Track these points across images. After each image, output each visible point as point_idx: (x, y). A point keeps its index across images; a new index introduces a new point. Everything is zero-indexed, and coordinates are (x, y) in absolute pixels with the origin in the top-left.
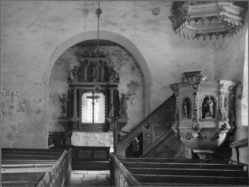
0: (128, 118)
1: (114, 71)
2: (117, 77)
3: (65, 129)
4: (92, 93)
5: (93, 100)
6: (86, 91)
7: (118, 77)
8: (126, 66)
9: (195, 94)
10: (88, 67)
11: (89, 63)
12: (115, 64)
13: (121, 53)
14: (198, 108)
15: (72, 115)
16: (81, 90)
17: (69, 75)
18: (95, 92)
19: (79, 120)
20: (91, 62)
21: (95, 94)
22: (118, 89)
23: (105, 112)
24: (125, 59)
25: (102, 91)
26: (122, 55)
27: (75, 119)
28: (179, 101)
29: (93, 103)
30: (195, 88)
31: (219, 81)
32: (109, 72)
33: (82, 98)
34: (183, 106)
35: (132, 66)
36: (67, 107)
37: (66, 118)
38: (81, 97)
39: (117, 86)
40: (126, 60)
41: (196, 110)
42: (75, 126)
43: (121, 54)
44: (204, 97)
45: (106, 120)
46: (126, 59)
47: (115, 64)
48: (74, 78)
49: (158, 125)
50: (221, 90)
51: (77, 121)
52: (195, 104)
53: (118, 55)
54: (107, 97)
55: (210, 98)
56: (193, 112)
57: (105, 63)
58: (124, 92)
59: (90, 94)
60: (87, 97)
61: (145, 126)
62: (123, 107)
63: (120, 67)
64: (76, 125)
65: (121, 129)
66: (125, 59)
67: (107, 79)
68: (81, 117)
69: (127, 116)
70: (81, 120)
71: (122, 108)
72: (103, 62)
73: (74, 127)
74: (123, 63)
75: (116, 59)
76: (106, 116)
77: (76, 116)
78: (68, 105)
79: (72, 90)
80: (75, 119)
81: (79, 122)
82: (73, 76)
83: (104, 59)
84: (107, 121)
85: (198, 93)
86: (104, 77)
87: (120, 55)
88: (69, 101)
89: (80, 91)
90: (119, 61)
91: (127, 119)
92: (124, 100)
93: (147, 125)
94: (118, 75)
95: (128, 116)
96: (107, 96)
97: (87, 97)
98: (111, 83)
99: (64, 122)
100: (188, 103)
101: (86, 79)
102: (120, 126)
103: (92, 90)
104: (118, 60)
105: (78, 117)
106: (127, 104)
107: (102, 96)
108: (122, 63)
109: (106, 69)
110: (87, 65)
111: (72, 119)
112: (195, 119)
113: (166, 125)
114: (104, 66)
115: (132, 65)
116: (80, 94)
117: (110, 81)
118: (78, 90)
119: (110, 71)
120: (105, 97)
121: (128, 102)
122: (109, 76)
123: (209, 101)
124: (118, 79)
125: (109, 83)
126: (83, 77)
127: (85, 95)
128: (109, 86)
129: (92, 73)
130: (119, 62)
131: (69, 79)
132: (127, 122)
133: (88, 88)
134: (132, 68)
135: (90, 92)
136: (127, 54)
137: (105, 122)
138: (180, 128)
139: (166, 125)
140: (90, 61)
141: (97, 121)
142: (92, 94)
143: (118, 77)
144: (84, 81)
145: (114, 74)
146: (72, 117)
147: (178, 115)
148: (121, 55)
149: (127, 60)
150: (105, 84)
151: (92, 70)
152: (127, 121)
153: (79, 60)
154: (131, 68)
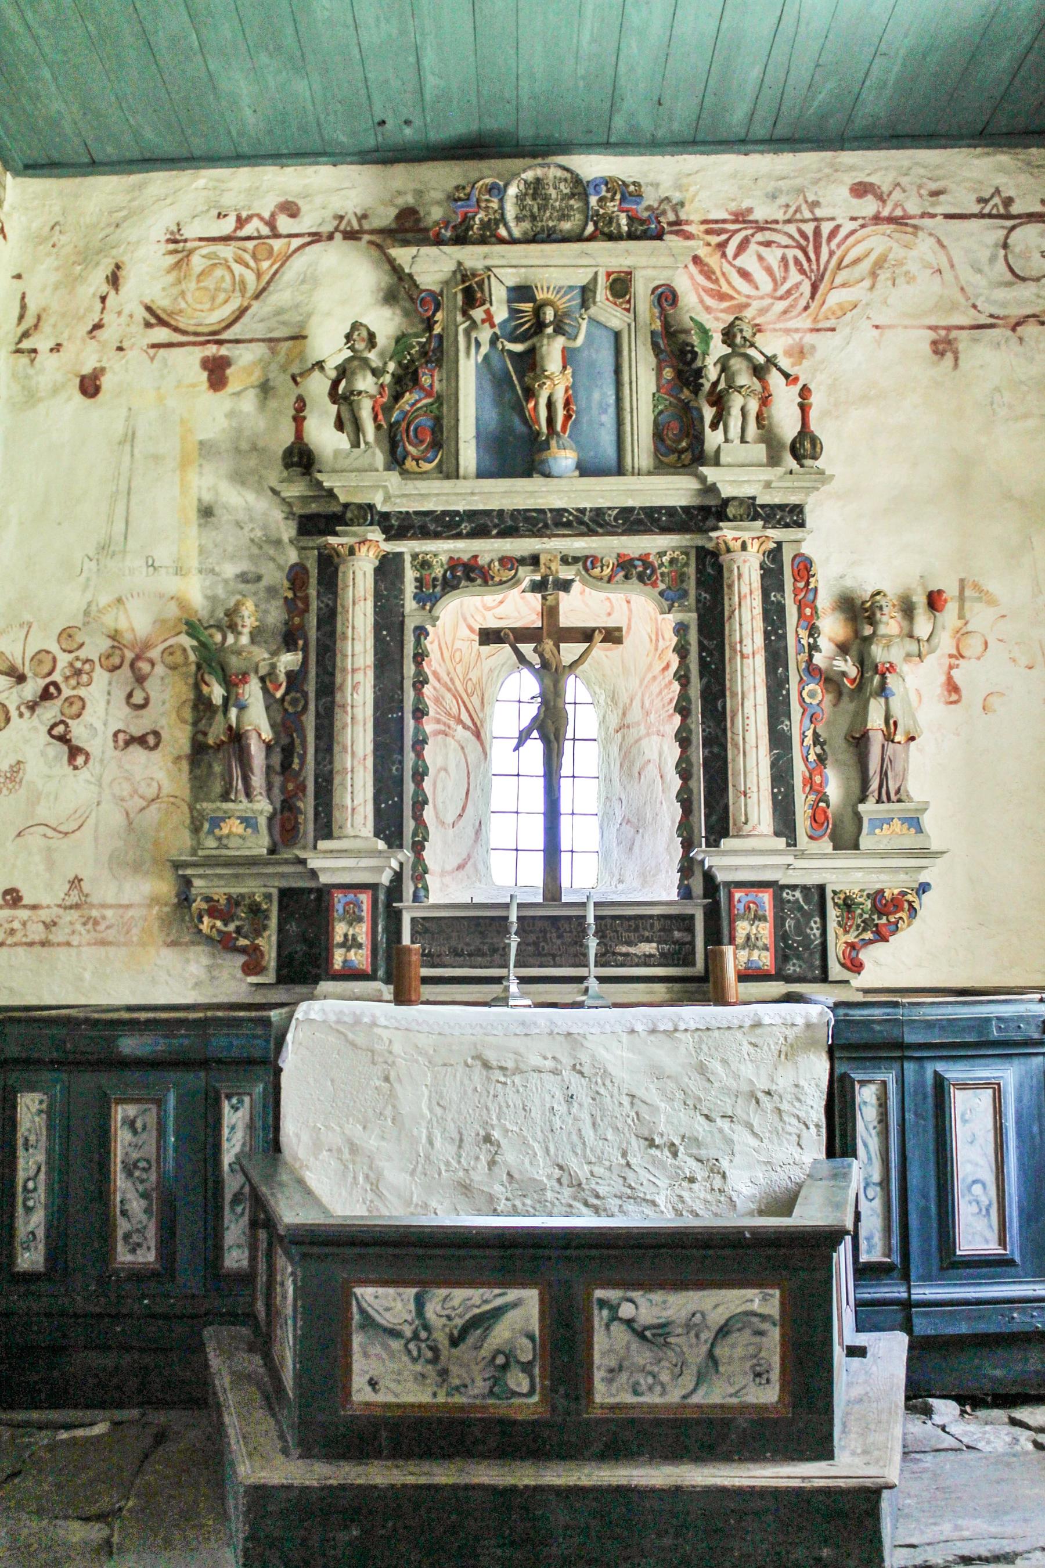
0: (934, 848)
2: (788, 427)
3: (249, 969)
4: (537, 587)
5: (551, 675)
6: (468, 574)
7: (805, 431)
8: (877, 327)
10: (485, 335)
11: (499, 294)
12: (763, 311)
13: (816, 204)
17: (299, 420)
18: (565, 586)
19: (398, 877)
20: (522, 293)
21: (579, 606)
22: (806, 549)
23: (677, 783)
24: (857, 261)
26: (826, 228)
27: (349, 855)
33: (430, 644)
35: (933, 328)
36: (267, 734)
37: (252, 862)
38: (421, 632)
39: (792, 516)
40: (874, 275)
42: (352, 938)
43: (816, 219)
45: (687, 867)
46: (866, 265)
47: (763, 311)
48: (342, 441)
51: (374, 887)
53: (792, 229)
54: (693, 636)
57: (666, 297)
58: (866, 581)
60: (489, 636)
62: (875, 720)
63: (810, 339)
64: (362, 932)
65: (856, 967)
66: (857, 261)
67: (682, 444)
68: (418, 848)
69: (915, 823)
70: (420, 871)
71: (859, 742)
72: (642, 290)
73: (343, 945)
74: (840, 306)
75: (769, 271)
76: (685, 829)
77: (367, 829)
78: (286, 725)
79: (330, 568)
80: (349, 855)
81: (395, 890)
82: (340, 425)
83: (649, 264)
84: (709, 878)
86: (658, 435)
87: (809, 228)
88: (295, 679)
89: (410, 575)
90: (797, 286)
91: (925, 853)
92: (878, 652)
94: (804, 408)
95: (926, 820)
96: (692, 618)
97: (489, 636)
99: (234, 902)
101: (469, 456)
102: (851, 938)
103: (534, 560)
104: (795, 276)
105: (381, 845)
106: (913, 697)
107: (649, 624)
108: (835, 298)
109: (677, 352)
110: (478, 314)
111: (314, 863)
114: (658, 325)
115: (933, 321)
116: (410, 605)
118: (388, 570)
120: (681, 629)
121: (915, 686)
122: (709, 413)
124: (805, 447)
125: (710, 472)
126: (440, 437)
127: (462, 614)
128: (710, 511)
129: (530, 393)
130: (806, 288)
131: (301, 459)
132: (924, 888)
133: (488, 549)
134: (934, 343)
135: (514, 581)
136: (877, 219)
137: (686, 893)
140: (511, 278)
141: (584, 879)
142: (535, 600)
143: (805, 431)
144: (450, 471)
146: (322, 845)
148: (817, 232)
149: (884, 275)
150: (675, 491)
151: (529, 363)
152: (924, 877)
153: (400, 289)
154: (927, 349)
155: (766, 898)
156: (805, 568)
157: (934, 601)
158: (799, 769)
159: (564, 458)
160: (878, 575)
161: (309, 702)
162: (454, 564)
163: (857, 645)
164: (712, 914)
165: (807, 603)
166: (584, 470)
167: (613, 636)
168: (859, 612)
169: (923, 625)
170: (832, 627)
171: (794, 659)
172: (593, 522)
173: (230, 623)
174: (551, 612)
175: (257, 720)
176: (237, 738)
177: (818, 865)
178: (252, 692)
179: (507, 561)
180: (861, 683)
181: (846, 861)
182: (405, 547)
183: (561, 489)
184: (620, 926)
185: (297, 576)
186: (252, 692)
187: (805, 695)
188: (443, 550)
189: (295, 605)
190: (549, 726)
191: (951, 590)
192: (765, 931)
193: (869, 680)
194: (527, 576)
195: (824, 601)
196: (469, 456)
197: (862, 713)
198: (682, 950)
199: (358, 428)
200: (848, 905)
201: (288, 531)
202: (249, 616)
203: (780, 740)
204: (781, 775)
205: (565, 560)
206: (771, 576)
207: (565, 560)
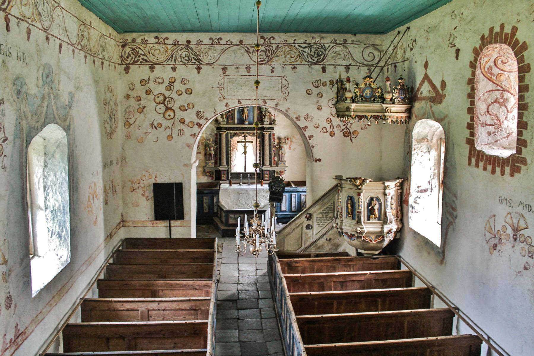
1: (269, 112)
6: (236, 135)
9: (359, 194)
14: (362, 211)
15: (220, 164)
16: (231, 133)
25: (254, 134)
28: (343, 197)
29: (245, 147)
30: (360, 189)
31: (384, 184)
32: (263, 113)
33: (232, 142)
34: (347, 204)
39: (273, 129)
41: (360, 212)
44: (369, 198)
48: (221, 120)
49: (320, 216)
50: (387, 191)
52: (359, 205)
55: (375, 199)
56: (357, 214)
59: (241, 138)
61: (306, 217)
62: (280, 153)
69: (284, 164)
71: (279, 155)
79: (220, 135)
85: (362, 194)
92: (281, 145)
93: (308, 216)
97: (238, 142)
98: (265, 126)
100: (352, 202)
101: (236, 121)
103: (243, 133)
112: (359, 222)
113: (330, 215)
117: (265, 123)
118: (227, 134)
119: (265, 111)
123: (374, 202)
124: (274, 121)
126: (233, 119)
127: (235, 139)
128: (263, 129)
138: (343, 227)
139: (330, 215)
144: (234, 124)
145: (269, 116)
147: (341, 213)
155: (268, 172)
156: (274, 134)
157: (288, 139)
158: (272, 157)
159: (247, 123)
160: (282, 136)
161: (218, 151)
162: (234, 133)
163: (279, 143)
164: (262, 173)
165: (274, 138)
166: (249, 124)
167: (252, 142)
168: (279, 139)
169: (287, 141)
170: (277, 141)
171: (272, 145)
172: (250, 129)
173: (209, 140)
174: (245, 139)
175: (213, 152)
176: (210, 154)
177: (274, 168)
178: (212, 149)
179: (240, 133)
180: (279, 148)
181: (277, 168)
182: (229, 131)
183: (246, 125)
184: (252, 174)
185: (216, 135)
186: (212, 149)
187: (273, 149)
188: (233, 132)
189: (216, 138)
190: (245, 152)
191: (289, 137)
192: (268, 176)
193: (280, 148)
194: (243, 135)
195: (276, 138)
196: (236, 121)
197: (279, 152)
198: (259, 177)
199: (223, 119)
200: (277, 172)
201: (215, 129)
202: (211, 140)
203: (270, 154)
204: (270, 158)
205: (247, 133)
206: (270, 136)
207: (247, 133)
